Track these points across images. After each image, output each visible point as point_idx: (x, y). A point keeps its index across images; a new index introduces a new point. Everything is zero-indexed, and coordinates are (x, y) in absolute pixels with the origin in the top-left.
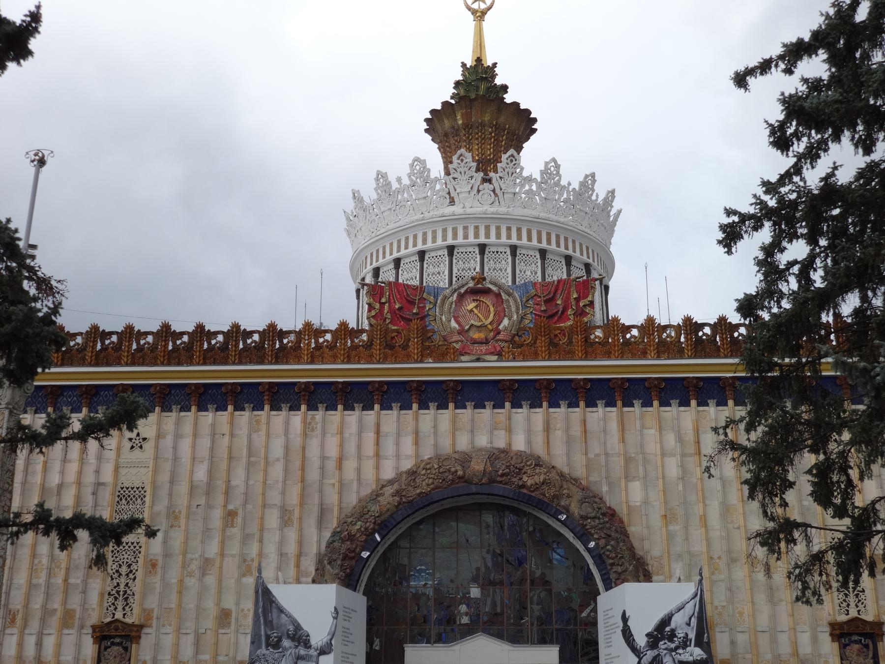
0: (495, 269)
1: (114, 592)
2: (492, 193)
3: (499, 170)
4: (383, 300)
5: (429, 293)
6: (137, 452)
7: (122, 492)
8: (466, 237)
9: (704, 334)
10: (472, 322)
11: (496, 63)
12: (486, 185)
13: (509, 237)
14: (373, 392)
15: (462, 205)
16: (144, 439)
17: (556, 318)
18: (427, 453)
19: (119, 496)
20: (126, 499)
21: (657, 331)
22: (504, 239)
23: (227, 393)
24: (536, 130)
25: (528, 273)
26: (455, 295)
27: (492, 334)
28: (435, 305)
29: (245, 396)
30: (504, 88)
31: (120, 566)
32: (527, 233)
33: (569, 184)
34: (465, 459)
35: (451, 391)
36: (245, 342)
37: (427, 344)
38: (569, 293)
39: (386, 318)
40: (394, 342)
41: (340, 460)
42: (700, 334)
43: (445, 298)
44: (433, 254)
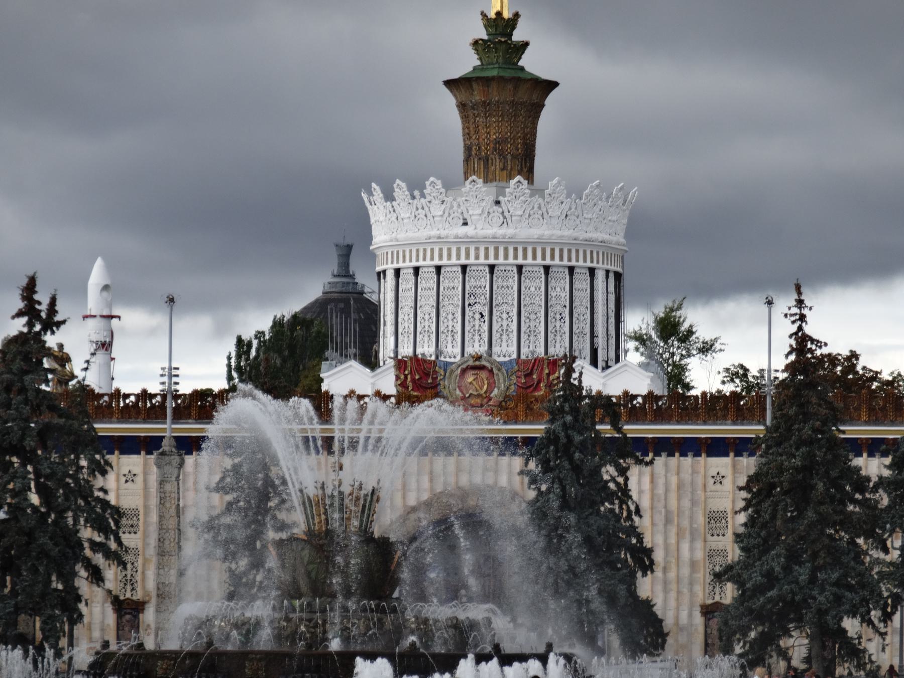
0: (503, 287)
2: (501, 216)
3: (508, 195)
4: (406, 372)
5: (440, 367)
8: (477, 258)
9: (637, 403)
10: (471, 391)
12: (496, 208)
13: (516, 257)
15: (474, 227)
17: (532, 388)
18: (439, 489)
22: (511, 260)
25: (533, 289)
26: (459, 370)
27: (485, 400)
38: (542, 369)
42: (635, 402)
43: (452, 372)
44: (449, 269)
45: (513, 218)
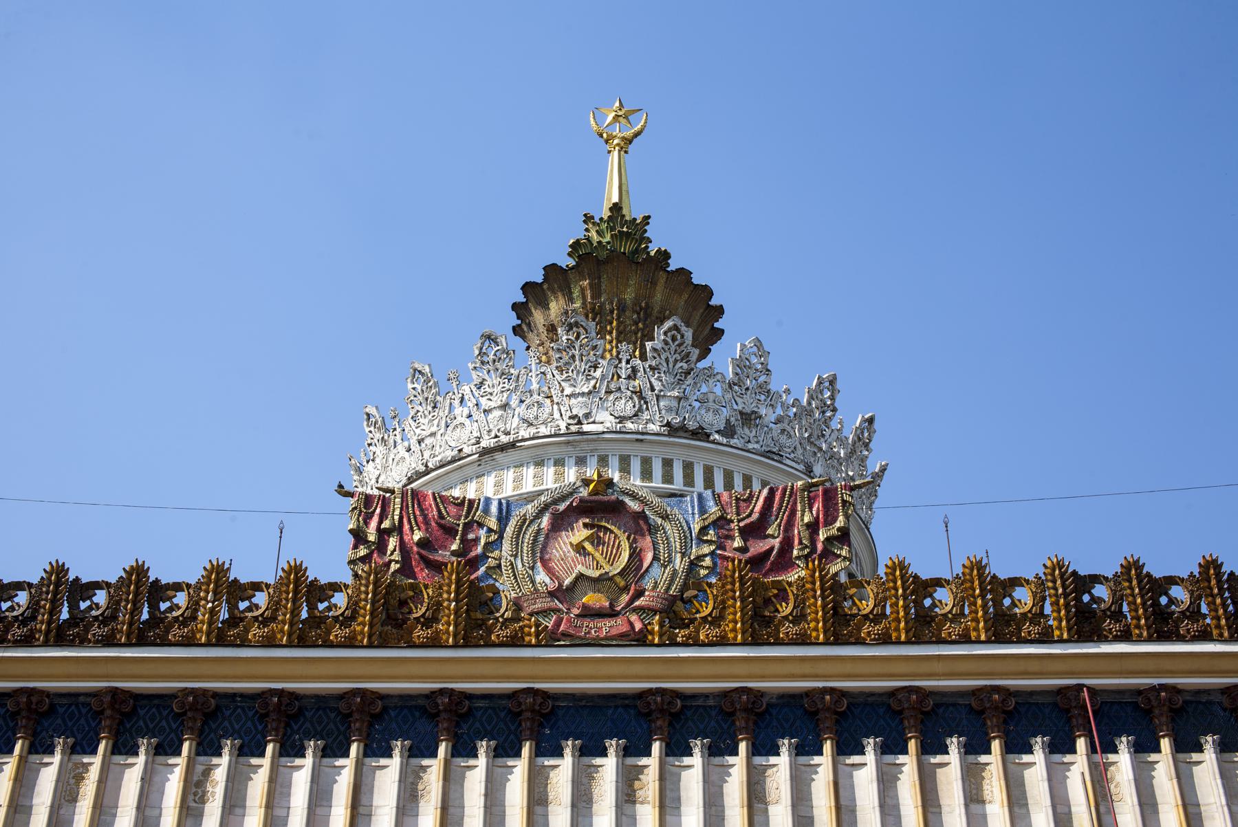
11: (649, 217)
14: (350, 715)
21: (991, 591)
23: (18, 713)
24: (722, 332)
28: (501, 537)
29: (59, 721)
30: (664, 256)
32: (705, 473)
33: (788, 391)
35: (528, 714)
36: (73, 607)
37: (479, 616)
38: (793, 513)
39: (390, 561)
40: (406, 610)
45: (662, 404)
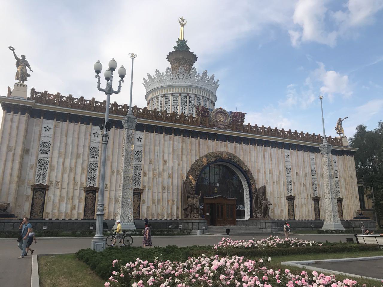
1: (90, 178)
6: (47, 132)
7: (42, 144)
16: (141, 139)
19: (41, 145)
20: (43, 146)
31: (136, 173)
34: (221, 153)
41: (191, 150)
